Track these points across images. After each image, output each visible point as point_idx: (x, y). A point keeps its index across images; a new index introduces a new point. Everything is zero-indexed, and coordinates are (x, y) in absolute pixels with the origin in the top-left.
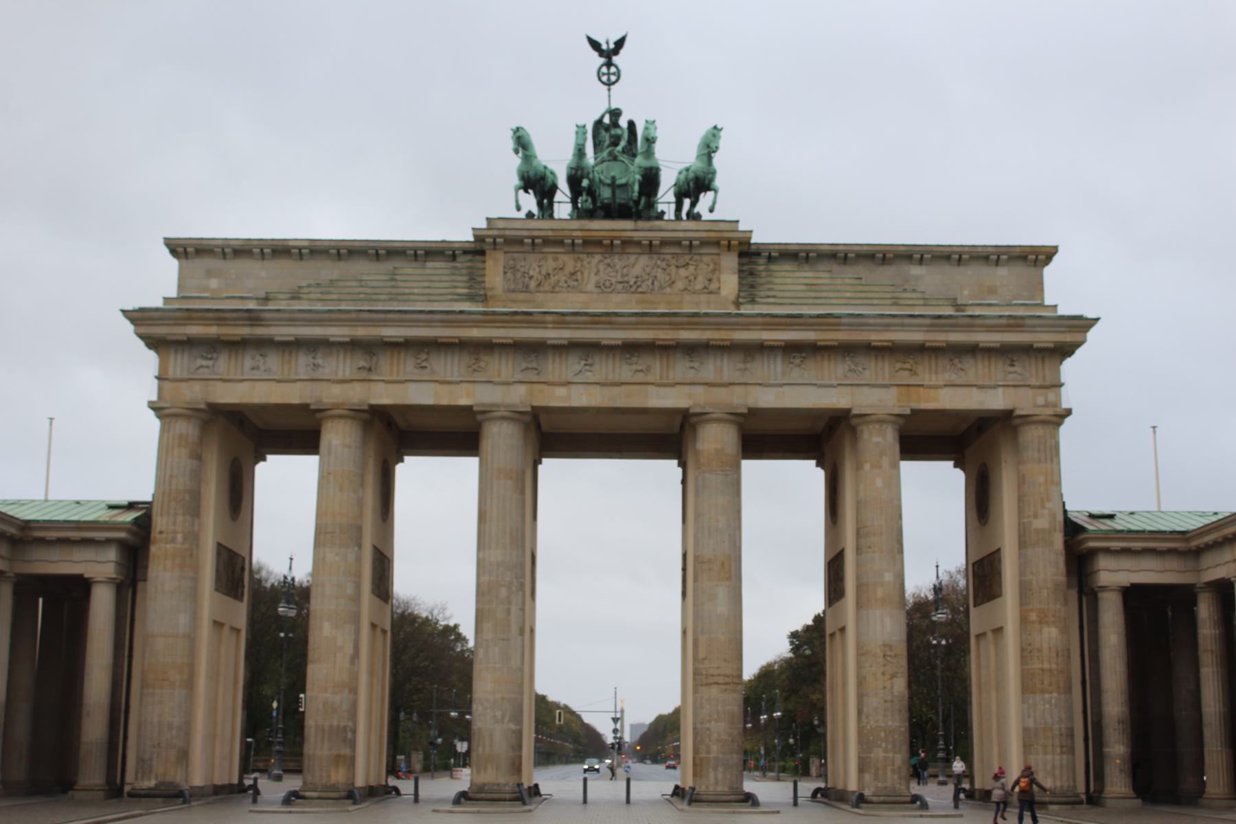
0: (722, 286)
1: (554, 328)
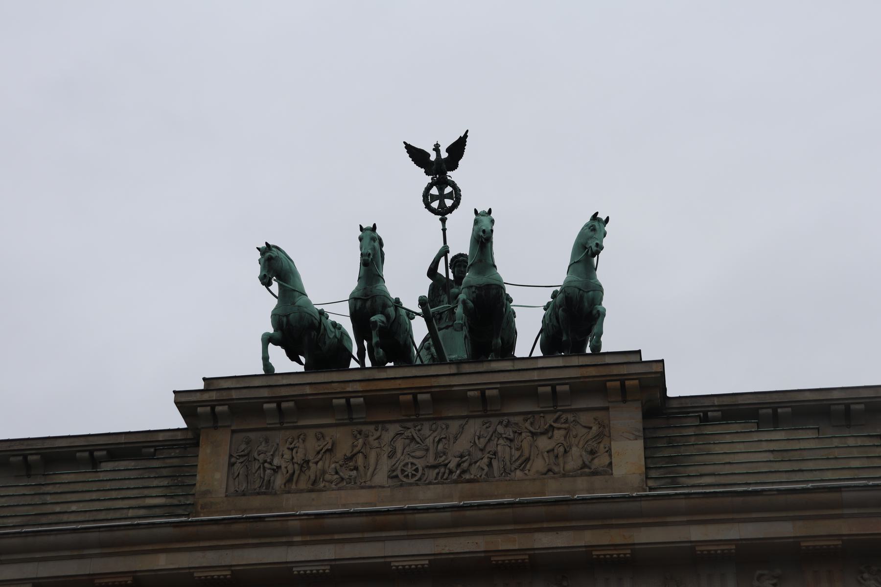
0: (613, 465)
1: (305, 543)
